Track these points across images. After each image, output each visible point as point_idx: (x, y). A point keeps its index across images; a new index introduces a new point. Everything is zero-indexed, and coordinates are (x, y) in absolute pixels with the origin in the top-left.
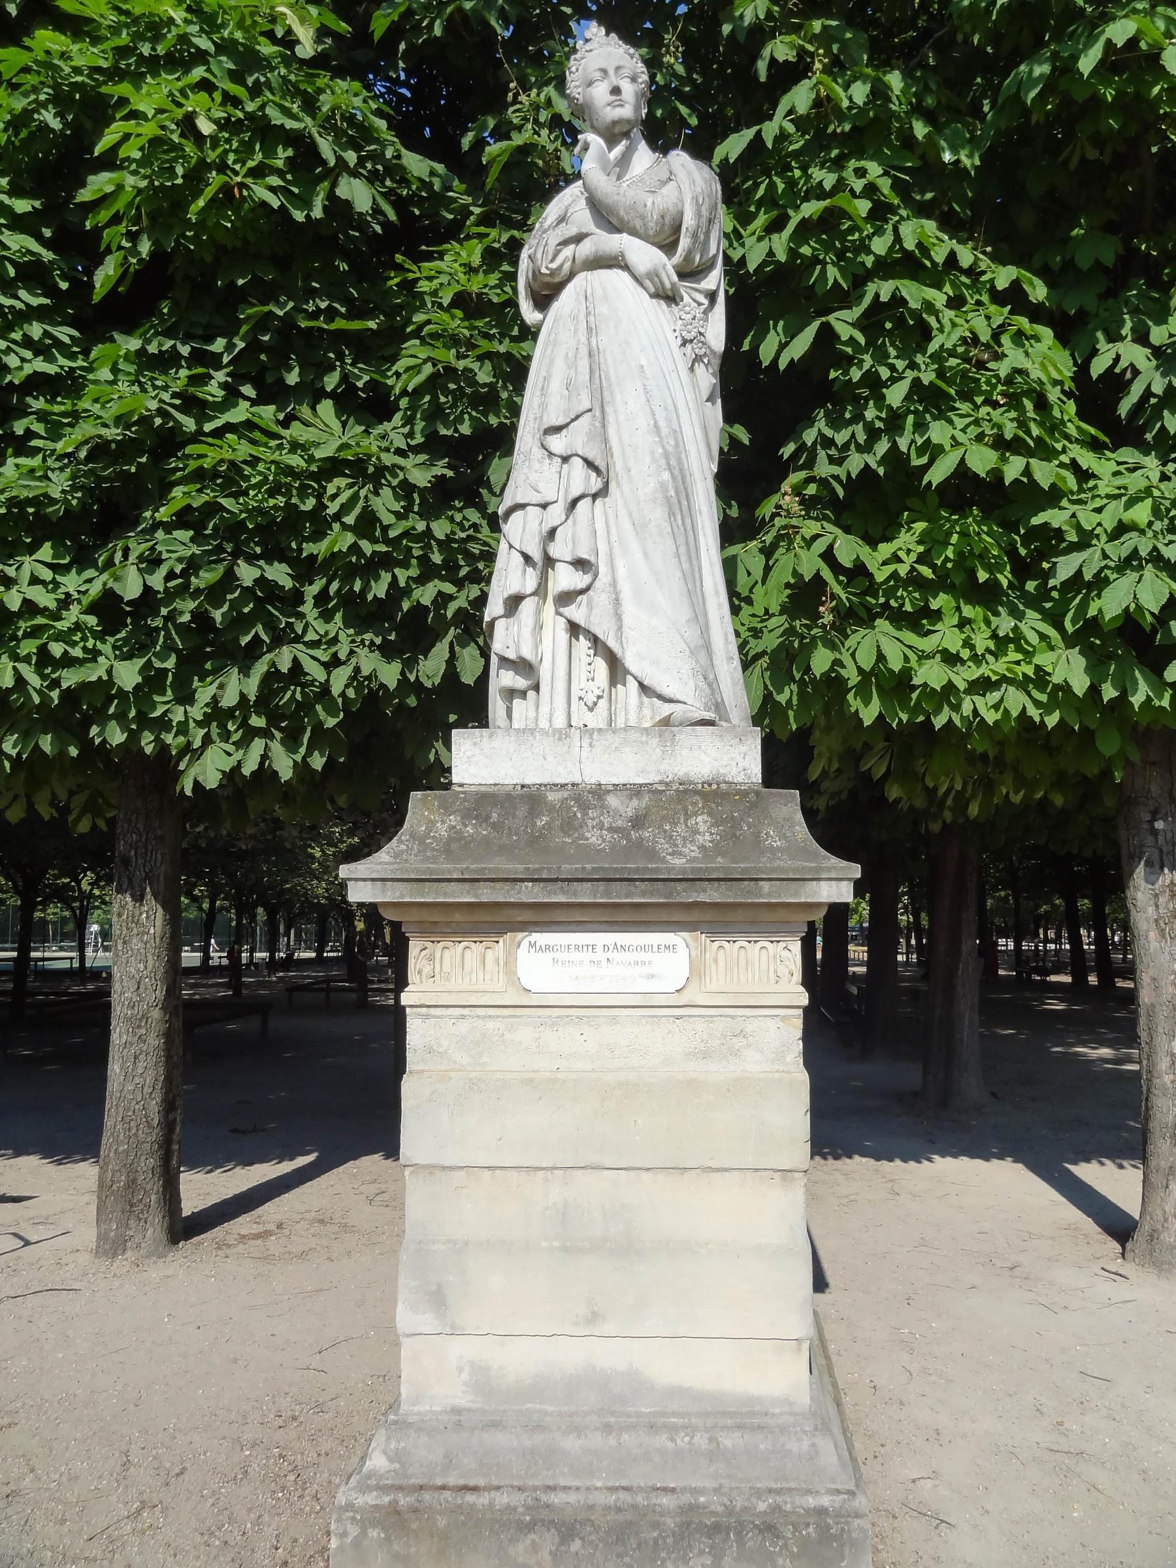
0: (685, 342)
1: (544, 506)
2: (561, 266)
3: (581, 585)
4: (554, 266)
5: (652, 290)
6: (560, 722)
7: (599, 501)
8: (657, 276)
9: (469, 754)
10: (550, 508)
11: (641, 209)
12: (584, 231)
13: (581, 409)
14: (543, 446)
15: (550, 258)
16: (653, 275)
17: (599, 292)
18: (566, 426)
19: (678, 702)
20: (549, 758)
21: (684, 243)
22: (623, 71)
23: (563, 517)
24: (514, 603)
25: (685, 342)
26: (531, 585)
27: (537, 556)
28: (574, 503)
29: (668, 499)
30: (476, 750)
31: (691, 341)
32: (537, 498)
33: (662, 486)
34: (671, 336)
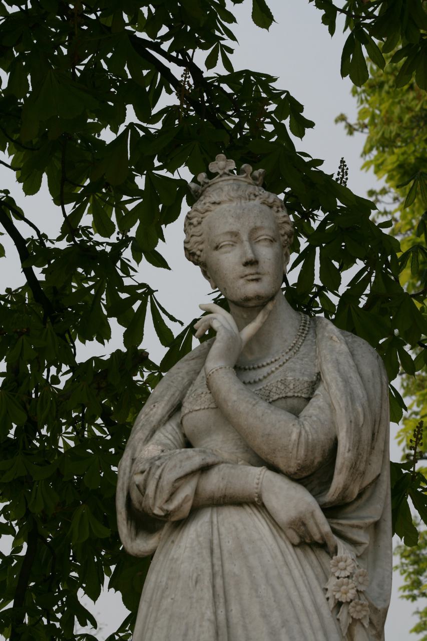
0: (339, 604)
4: (171, 507)
5: (297, 540)
8: (304, 524)
12: (210, 460)
15: (165, 496)
17: (228, 544)
21: (339, 480)
22: (260, 233)
31: (348, 603)
34: (320, 598)
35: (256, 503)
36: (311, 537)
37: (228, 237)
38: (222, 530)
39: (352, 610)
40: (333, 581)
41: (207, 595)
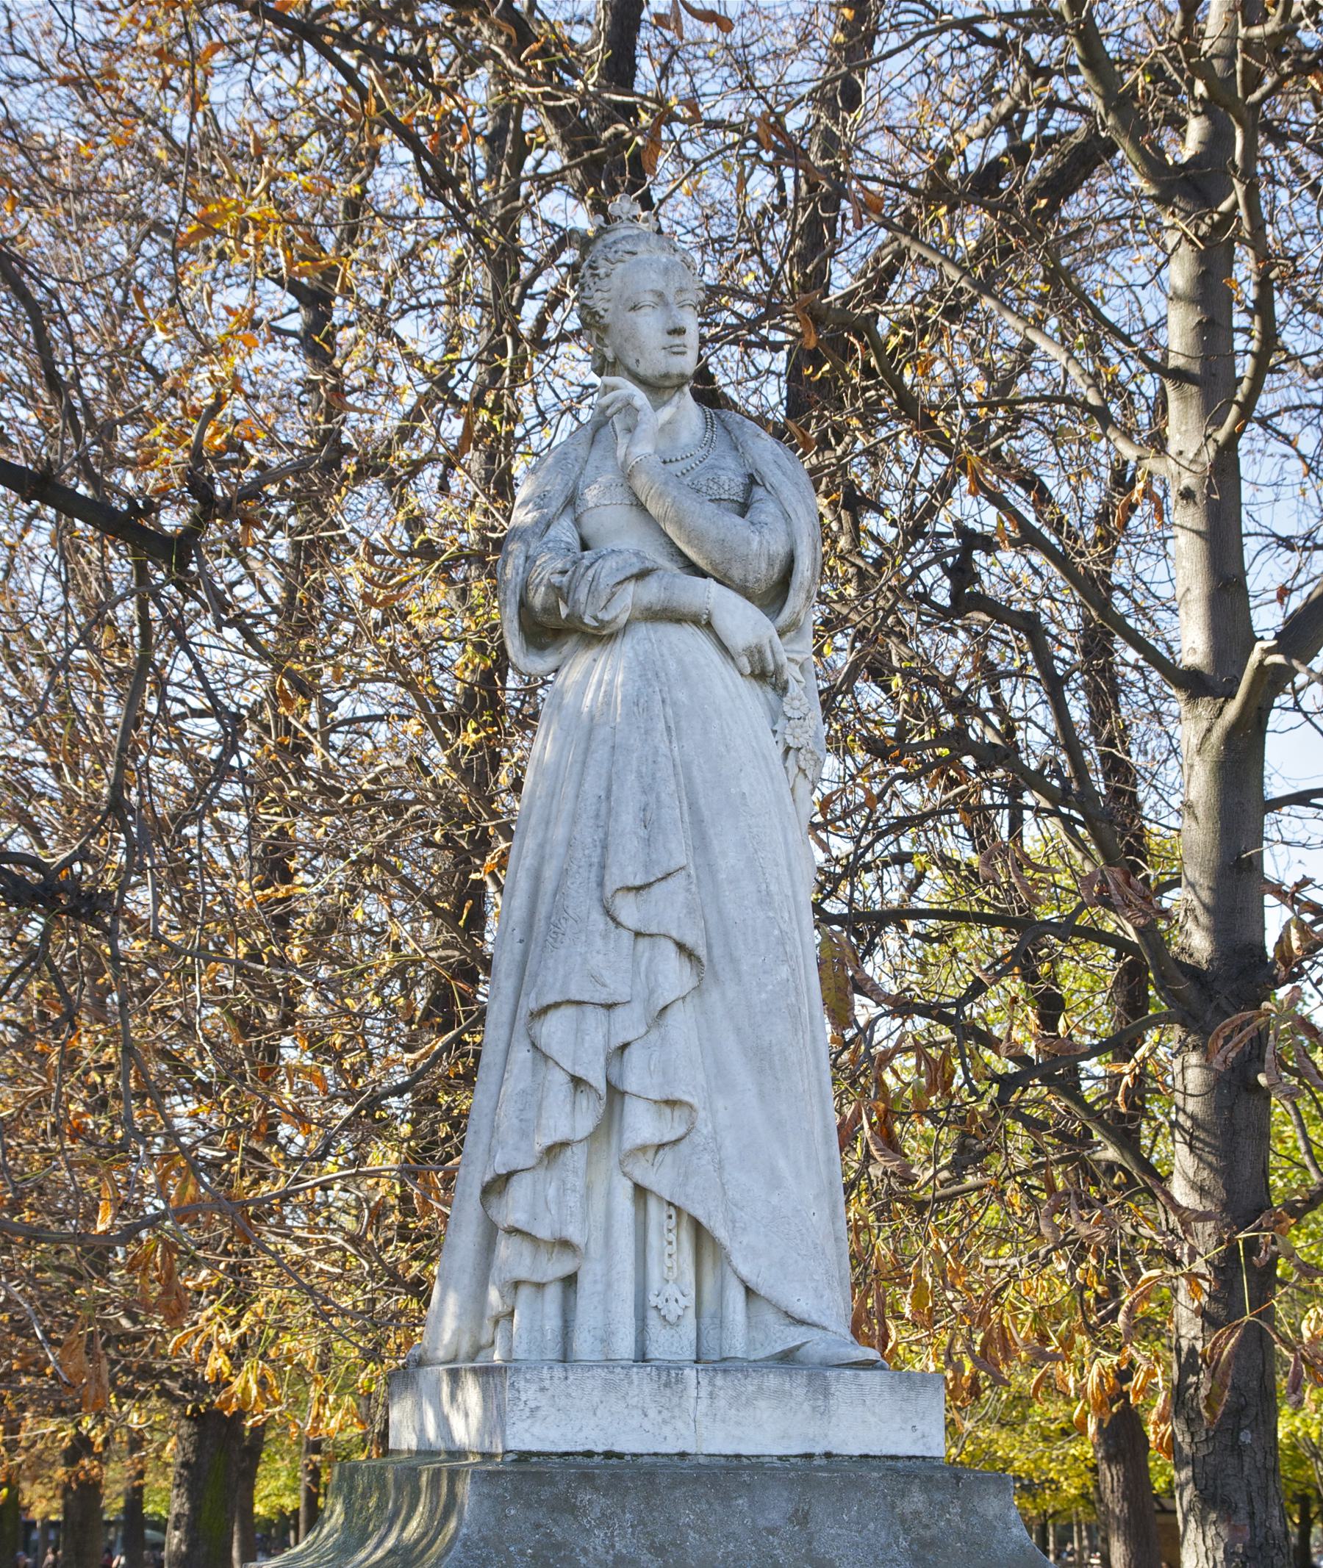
1: (609, 1007)
4: (606, 616)
5: (748, 670)
6: (625, 1346)
9: (532, 1404)
10: (619, 1011)
12: (648, 565)
13: (673, 866)
16: (756, 653)
18: (649, 885)
20: (652, 1413)
22: (686, 296)
23: (642, 1030)
24: (555, 1151)
27: (597, 1079)
35: (706, 624)
40: (782, 721)
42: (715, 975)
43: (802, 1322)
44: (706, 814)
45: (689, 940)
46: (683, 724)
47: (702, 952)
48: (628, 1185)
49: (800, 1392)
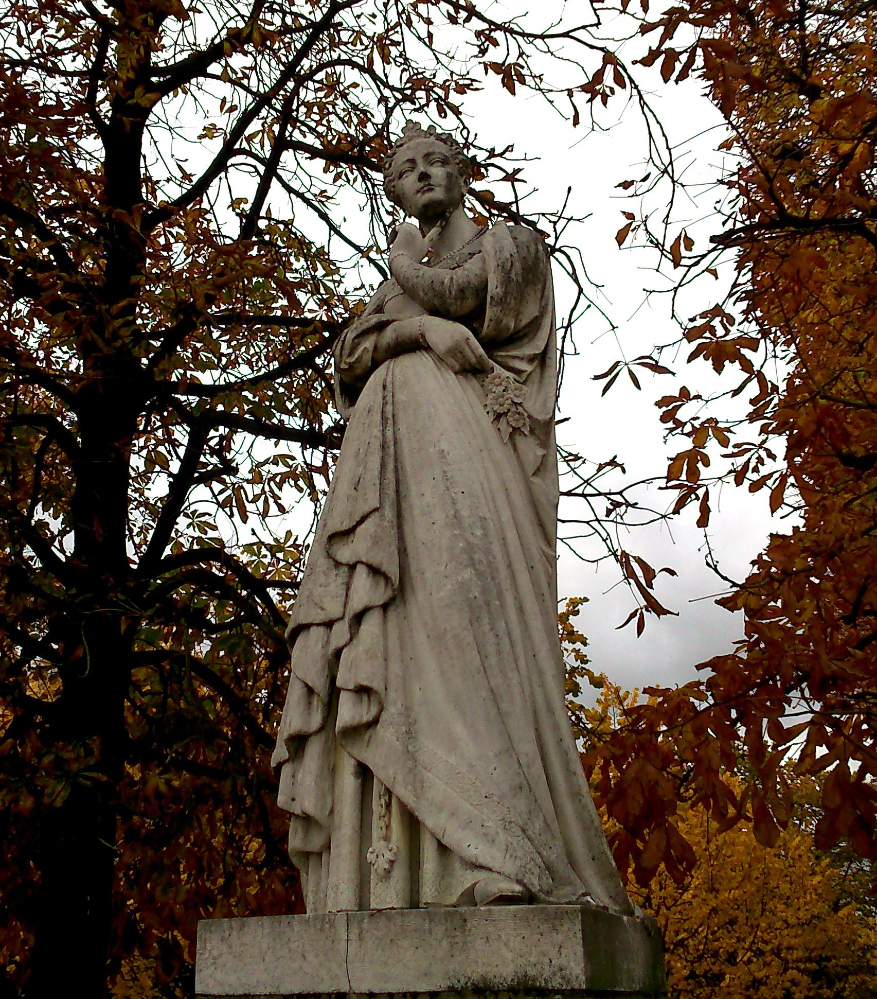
0: (498, 417)
1: (329, 625)
2: (360, 357)
3: (366, 718)
4: (352, 360)
5: (457, 367)
7: (391, 614)
9: (215, 953)
10: (336, 627)
11: (437, 286)
13: (367, 509)
14: (329, 556)
16: (455, 351)
19: (481, 867)
20: (310, 957)
24: (298, 742)
25: (498, 417)
26: (316, 720)
28: (358, 618)
29: (470, 604)
30: (224, 948)
31: (506, 414)
32: (321, 617)
33: (464, 587)
34: (481, 412)
36: (470, 363)
37: (408, 165)
38: (397, 372)
39: (510, 419)
41: (378, 417)
42: (412, 587)
43: (481, 867)
44: (409, 469)
45: (375, 562)
46: (400, 415)
47: (393, 571)
48: (353, 761)
49: (439, 931)
